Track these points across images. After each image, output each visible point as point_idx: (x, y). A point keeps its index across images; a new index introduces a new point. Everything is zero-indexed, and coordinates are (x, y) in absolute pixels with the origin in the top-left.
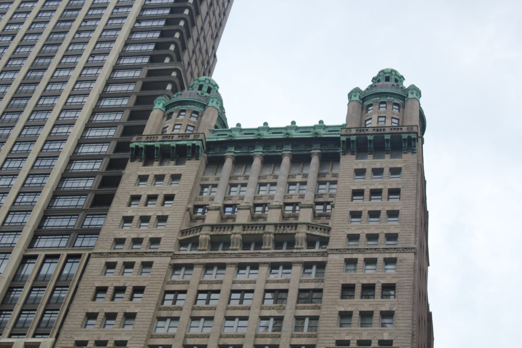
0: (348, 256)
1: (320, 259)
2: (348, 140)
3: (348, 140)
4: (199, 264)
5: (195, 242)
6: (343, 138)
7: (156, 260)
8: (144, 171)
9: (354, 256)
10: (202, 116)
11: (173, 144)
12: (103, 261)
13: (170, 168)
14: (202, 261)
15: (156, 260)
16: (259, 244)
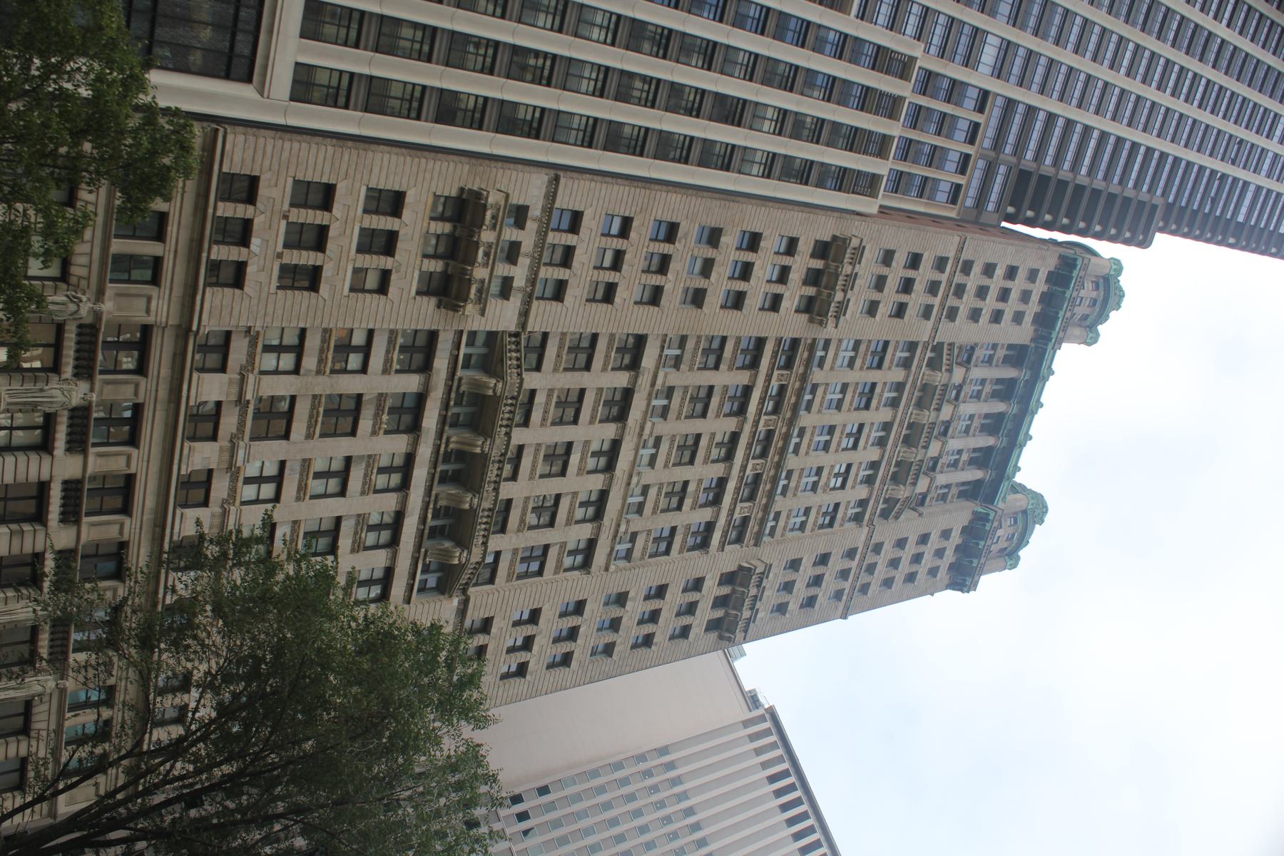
0: (859, 551)
1: (867, 517)
2: (988, 521)
3: (988, 521)
4: (907, 377)
5: (934, 364)
6: (992, 515)
7: (930, 324)
8: (1042, 276)
9: (858, 557)
10: (1080, 326)
11: (1061, 314)
12: (951, 255)
13: (1033, 307)
14: (911, 379)
15: (930, 324)
16: (908, 441)
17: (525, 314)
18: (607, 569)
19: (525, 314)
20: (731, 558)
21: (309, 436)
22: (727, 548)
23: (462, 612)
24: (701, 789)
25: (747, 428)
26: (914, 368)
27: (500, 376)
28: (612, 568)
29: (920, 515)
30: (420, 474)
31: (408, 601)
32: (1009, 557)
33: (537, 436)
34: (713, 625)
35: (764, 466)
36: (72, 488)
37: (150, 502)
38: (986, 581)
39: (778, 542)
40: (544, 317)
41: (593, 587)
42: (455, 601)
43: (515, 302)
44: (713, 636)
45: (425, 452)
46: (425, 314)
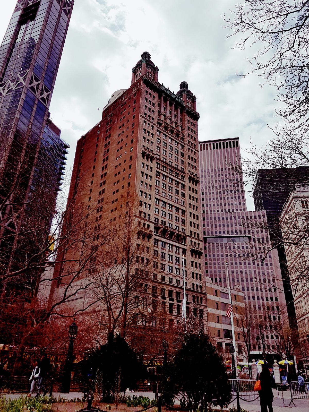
9: (190, 148)
12: (143, 119)
17: (152, 222)
18: (186, 207)
19: (152, 222)
20: (187, 180)
21: (165, 261)
22: (185, 180)
23: (189, 236)
24: (207, 153)
25: (169, 175)
26: (161, 131)
27: (160, 228)
28: (185, 206)
29: (184, 129)
30: (171, 242)
31: (186, 246)
32: (193, 99)
33: (167, 220)
34: (196, 185)
35: (174, 172)
36: (170, 300)
37: (172, 288)
38: (198, 111)
39: (185, 168)
40: (152, 219)
41: (189, 210)
42: (188, 237)
43: (151, 224)
44: (198, 184)
45: (168, 241)
46: (152, 241)
